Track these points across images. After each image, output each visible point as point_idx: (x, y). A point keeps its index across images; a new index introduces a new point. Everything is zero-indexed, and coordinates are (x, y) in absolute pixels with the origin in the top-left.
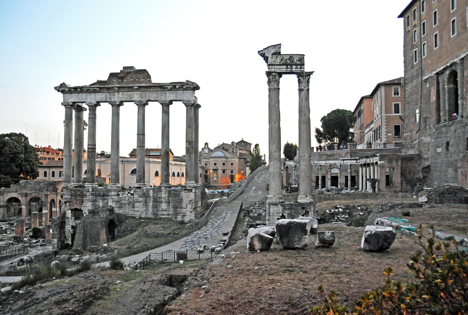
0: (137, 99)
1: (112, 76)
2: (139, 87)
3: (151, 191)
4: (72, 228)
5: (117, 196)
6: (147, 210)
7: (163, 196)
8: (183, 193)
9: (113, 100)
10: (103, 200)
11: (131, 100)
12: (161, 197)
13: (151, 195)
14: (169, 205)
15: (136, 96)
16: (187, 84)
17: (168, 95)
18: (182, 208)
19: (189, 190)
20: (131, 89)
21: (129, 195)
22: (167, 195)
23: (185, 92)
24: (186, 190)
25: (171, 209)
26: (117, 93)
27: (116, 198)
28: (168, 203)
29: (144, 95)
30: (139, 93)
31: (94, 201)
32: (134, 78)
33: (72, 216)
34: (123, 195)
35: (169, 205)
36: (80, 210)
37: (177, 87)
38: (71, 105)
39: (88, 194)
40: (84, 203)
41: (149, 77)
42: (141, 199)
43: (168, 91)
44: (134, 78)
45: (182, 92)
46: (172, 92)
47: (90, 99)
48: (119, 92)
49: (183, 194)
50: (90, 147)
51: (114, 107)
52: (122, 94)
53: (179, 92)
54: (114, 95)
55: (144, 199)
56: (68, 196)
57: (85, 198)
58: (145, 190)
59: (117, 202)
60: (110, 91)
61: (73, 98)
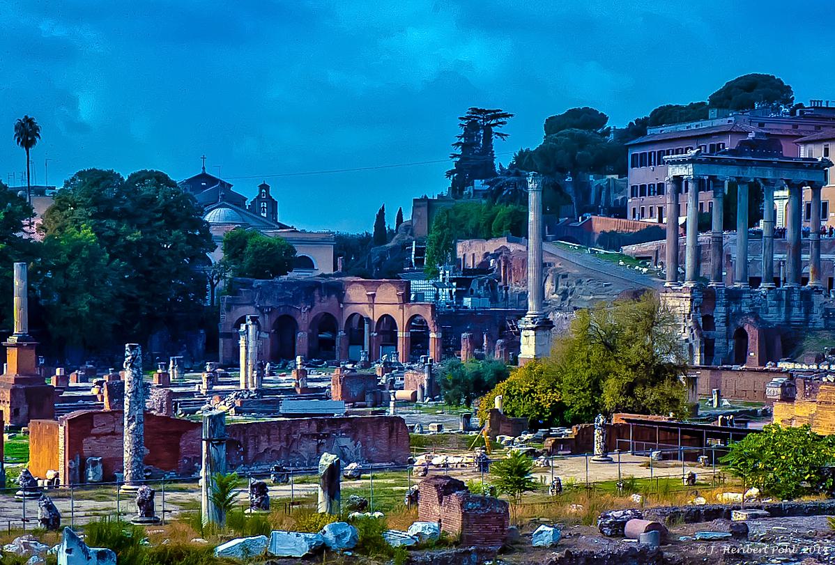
6: (780, 316)
7: (795, 299)
10: (736, 303)
13: (784, 298)
14: (800, 310)
18: (813, 313)
21: (762, 297)
25: (803, 315)
27: (750, 301)
28: (800, 307)
31: (727, 306)
35: (800, 310)
40: (717, 308)
49: (815, 297)
54: (747, 169)
59: (751, 306)
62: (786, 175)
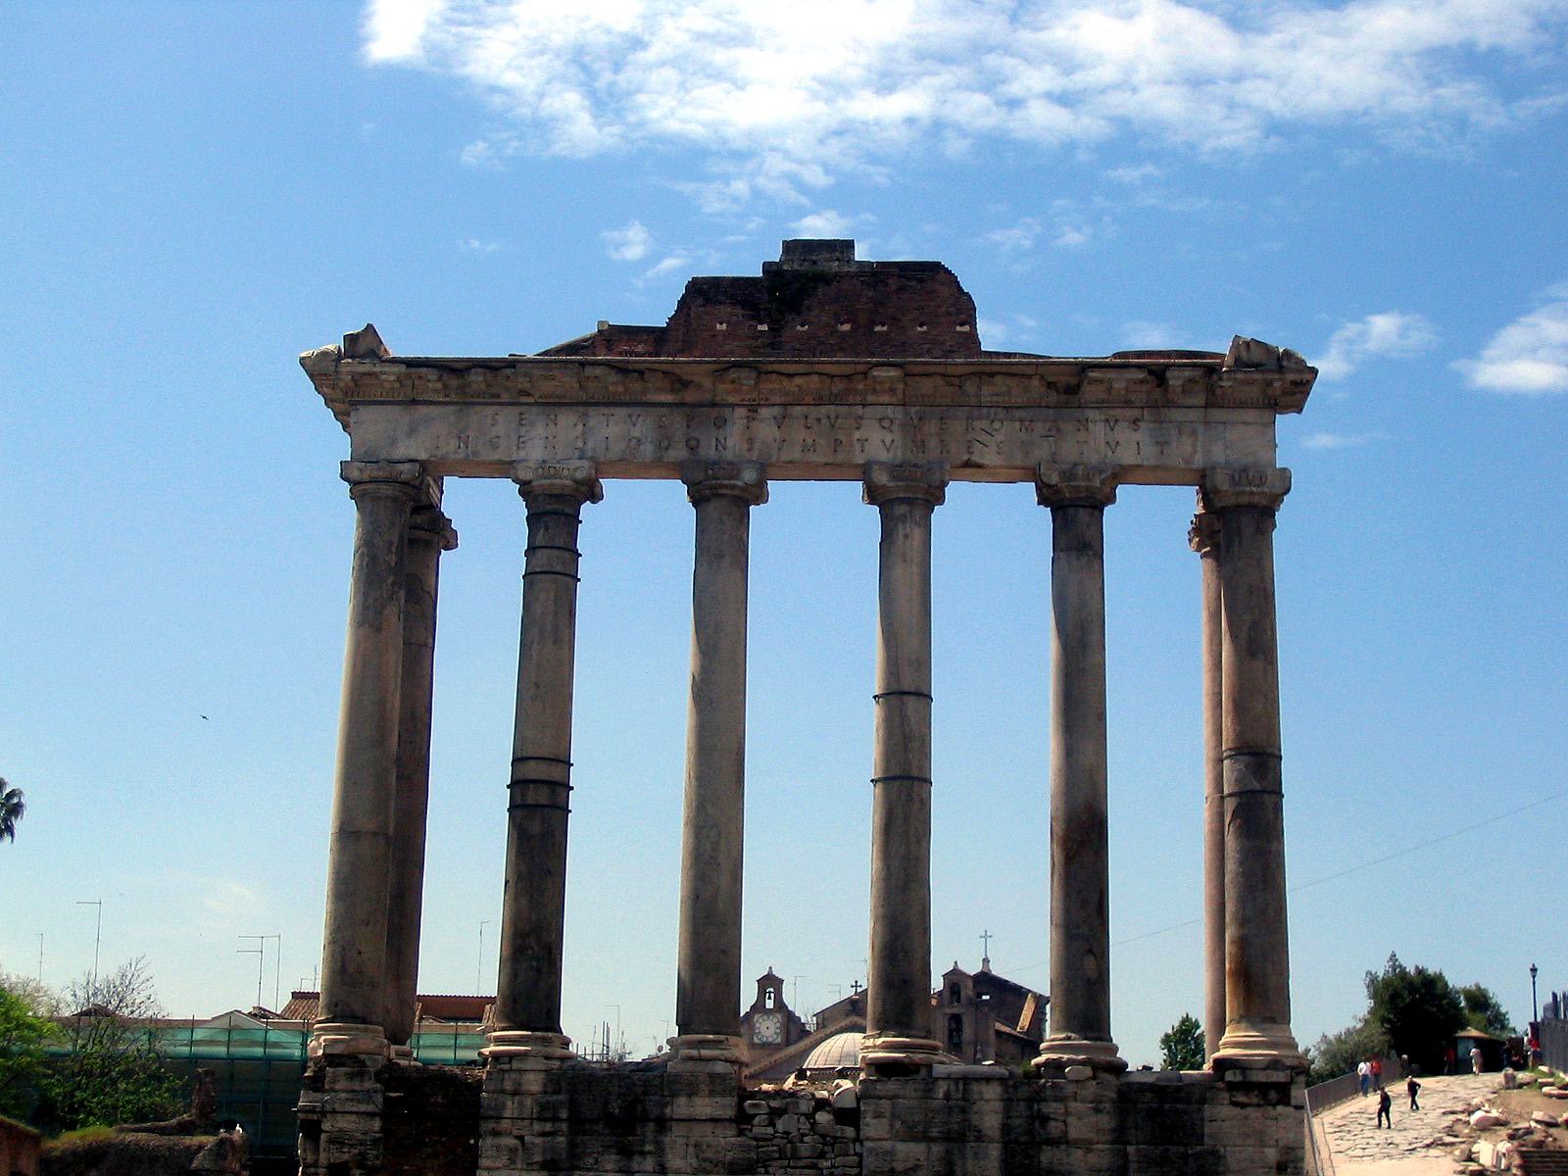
0: (884, 456)
1: (708, 301)
3: (992, 1091)
5: (731, 1131)
7: (1077, 1129)
8: (1226, 1110)
9: (709, 451)
10: (626, 1152)
11: (841, 457)
12: (1062, 1141)
15: (879, 442)
16: (1239, 363)
17: (1098, 430)
19: (1263, 1088)
20: (839, 386)
22: (1106, 1121)
24: (1246, 1087)
26: (741, 412)
29: (931, 427)
34: (780, 1125)
37: (1175, 379)
38: (405, 483)
39: (511, 1107)
41: (964, 309)
42: (918, 1149)
43: (1100, 405)
44: (862, 318)
45: (1193, 415)
46: (1136, 413)
47: (549, 443)
48: (753, 408)
50: (535, 771)
51: (713, 508)
52: (780, 422)
53: (1176, 415)
54: (721, 423)
55: (937, 1149)
56: (364, 1124)
57: (489, 1141)
58: (941, 1089)
60: (690, 396)
61: (413, 440)
62: (996, 439)
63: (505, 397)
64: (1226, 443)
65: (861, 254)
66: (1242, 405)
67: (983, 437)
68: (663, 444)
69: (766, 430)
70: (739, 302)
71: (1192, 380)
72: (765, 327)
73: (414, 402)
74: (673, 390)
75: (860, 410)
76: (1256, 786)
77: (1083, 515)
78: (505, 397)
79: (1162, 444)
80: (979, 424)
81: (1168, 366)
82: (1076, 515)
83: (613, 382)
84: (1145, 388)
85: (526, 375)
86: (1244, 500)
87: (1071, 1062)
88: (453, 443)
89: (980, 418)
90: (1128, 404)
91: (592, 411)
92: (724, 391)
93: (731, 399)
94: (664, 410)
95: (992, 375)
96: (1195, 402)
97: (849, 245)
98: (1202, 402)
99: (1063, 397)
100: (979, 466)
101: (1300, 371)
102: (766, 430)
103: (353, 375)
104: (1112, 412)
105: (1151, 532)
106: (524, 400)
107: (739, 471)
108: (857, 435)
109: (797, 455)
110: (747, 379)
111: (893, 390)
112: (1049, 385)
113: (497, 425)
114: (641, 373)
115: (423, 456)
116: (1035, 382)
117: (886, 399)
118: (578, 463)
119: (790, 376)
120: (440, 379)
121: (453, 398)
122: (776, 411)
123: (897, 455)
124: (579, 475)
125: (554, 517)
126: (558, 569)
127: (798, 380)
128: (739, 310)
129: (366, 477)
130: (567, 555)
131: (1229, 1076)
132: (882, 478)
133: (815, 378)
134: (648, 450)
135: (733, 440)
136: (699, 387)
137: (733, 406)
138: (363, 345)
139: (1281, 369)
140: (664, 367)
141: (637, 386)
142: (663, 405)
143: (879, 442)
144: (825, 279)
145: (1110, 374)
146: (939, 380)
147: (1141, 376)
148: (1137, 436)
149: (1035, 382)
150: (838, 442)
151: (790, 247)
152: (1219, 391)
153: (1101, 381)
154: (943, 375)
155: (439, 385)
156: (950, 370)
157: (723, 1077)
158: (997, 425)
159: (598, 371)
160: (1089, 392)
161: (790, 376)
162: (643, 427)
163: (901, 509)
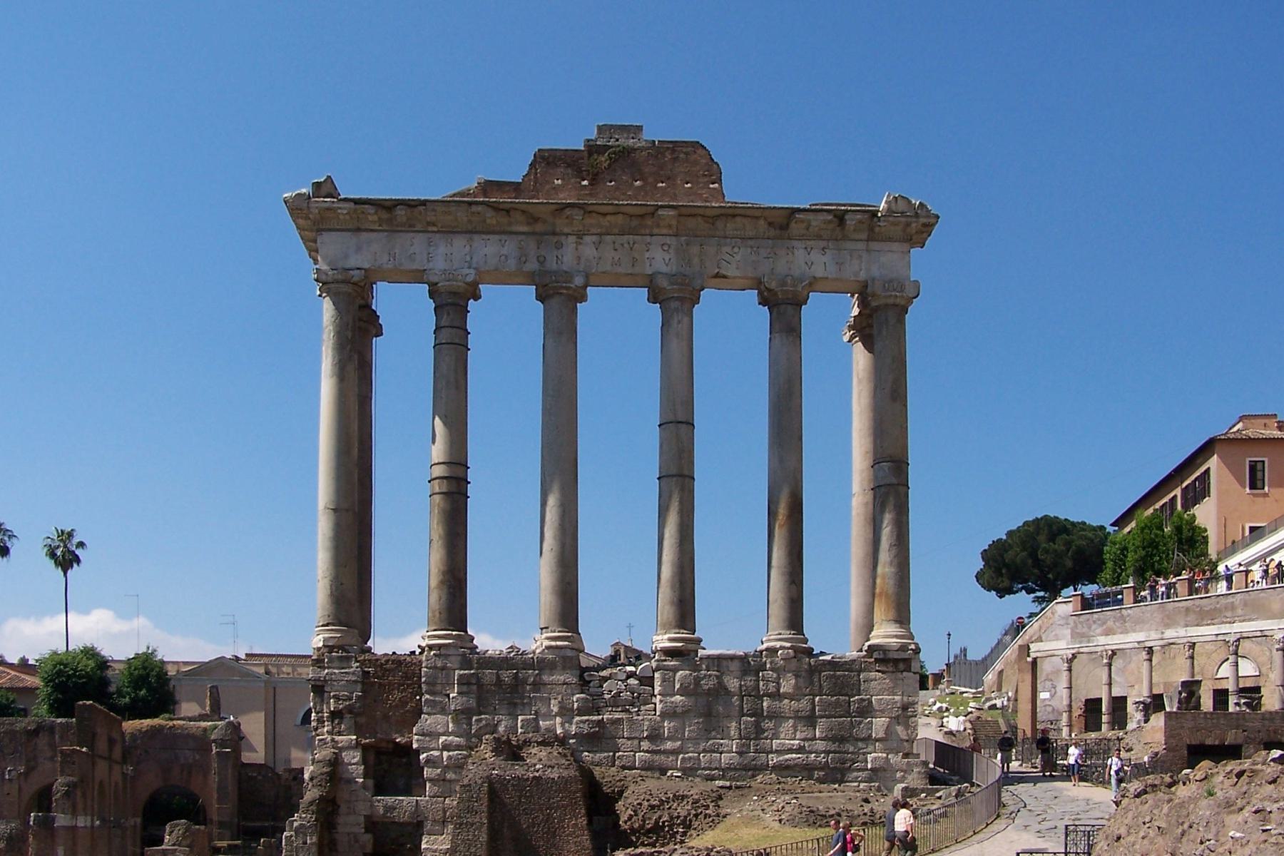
0: (664, 269)
2: (685, 213)
3: (735, 666)
4: (367, 831)
9: (552, 265)
11: (637, 270)
15: (660, 258)
17: (800, 254)
19: (896, 661)
20: (635, 223)
23: (875, 245)
25: (821, 745)
26: (572, 239)
29: (695, 249)
30: (671, 241)
32: (650, 180)
33: (366, 776)
36: (408, 753)
37: (851, 221)
41: (713, 172)
43: (801, 238)
45: (861, 245)
46: (822, 244)
48: (580, 236)
51: (555, 302)
53: (849, 245)
54: (559, 246)
60: (539, 227)
61: (363, 253)
62: (736, 260)
63: (419, 227)
64: (879, 263)
65: (647, 135)
66: (890, 239)
67: (727, 257)
68: (522, 258)
69: (589, 251)
70: (569, 166)
71: (860, 222)
72: (585, 183)
73: (358, 230)
74: (529, 224)
75: (648, 239)
76: (894, 481)
77: (790, 309)
78: (419, 227)
79: (840, 264)
80: (725, 249)
81: (847, 211)
82: (784, 307)
83: (491, 218)
84: (831, 226)
85: (434, 210)
86: (891, 301)
87: (782, 648)
88: (386, 258)
89: (726, 245)
90: (819, 237)
91: (476, 237)
92: (561, 224)
93: (566, 230)
94: (523, 237)
95: (734, 216)
96: (856, 236)
97: (640, 128)
98: (864, 236)
99: (778, 232)
100: (725, 277)
101: (928, 217)
102: (589, 251)
103: (319, 214)
104: (809, 243)
105: (829, 317)
106: (430, 229)
107: (572, 277)
108: (647, 255)
109: (608, 268)
110: (577, 215)
111: (670, 226)
112: (770, 224)
113: (414, 247)
114: (508, 211)
115: (366, 266)
116: (762, 222)
117: (665, 231)
118: (468, 271)
119: (605, 215)
120: (376, 213)
121: (385, 227)
122: (594, 238)
123: (673, 268)
124: (470, 279)
125: (452, 305)
126: (457, 341)
127: (609, 218)
128: (570, 171)
129: (330, 279)
130: (461, 332)
131: (876, 655)
132: (663, 283)
133: (620, 217)
134: (512, 264)
135: (570, 256)
136: (545, 222)
137: (567, 234)
138: (325, 188)
139: (917, 215)
140: (523, 207)
141: (505, 220)
142: (523, 233)
143: (660, 258)
144: (627, 152)
145: (811, 216)
146: (700, 219)
147: (830, 217)
148: (824, 259)
149: (762, 222)
150: (634, 260)
151: (601, 129)
152: (877, 229)
153: (802, 221)
154: (703, 216)
155: (375, 218)
156: (708, 213)
157: (571, 658)
158: (736, 250)
159: (480, 208)
160: (795, 228)
161: (605, 215)
162: (510, 247)
163: (674, 304)
